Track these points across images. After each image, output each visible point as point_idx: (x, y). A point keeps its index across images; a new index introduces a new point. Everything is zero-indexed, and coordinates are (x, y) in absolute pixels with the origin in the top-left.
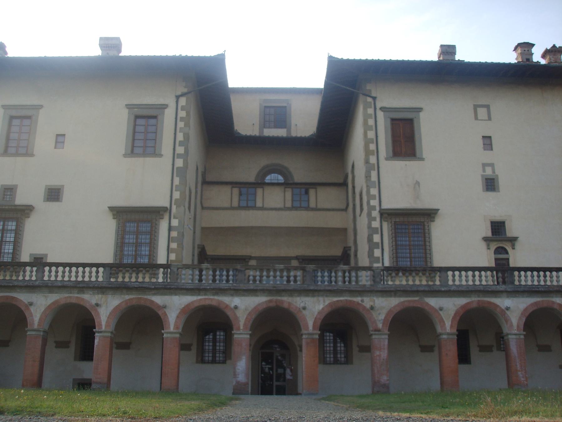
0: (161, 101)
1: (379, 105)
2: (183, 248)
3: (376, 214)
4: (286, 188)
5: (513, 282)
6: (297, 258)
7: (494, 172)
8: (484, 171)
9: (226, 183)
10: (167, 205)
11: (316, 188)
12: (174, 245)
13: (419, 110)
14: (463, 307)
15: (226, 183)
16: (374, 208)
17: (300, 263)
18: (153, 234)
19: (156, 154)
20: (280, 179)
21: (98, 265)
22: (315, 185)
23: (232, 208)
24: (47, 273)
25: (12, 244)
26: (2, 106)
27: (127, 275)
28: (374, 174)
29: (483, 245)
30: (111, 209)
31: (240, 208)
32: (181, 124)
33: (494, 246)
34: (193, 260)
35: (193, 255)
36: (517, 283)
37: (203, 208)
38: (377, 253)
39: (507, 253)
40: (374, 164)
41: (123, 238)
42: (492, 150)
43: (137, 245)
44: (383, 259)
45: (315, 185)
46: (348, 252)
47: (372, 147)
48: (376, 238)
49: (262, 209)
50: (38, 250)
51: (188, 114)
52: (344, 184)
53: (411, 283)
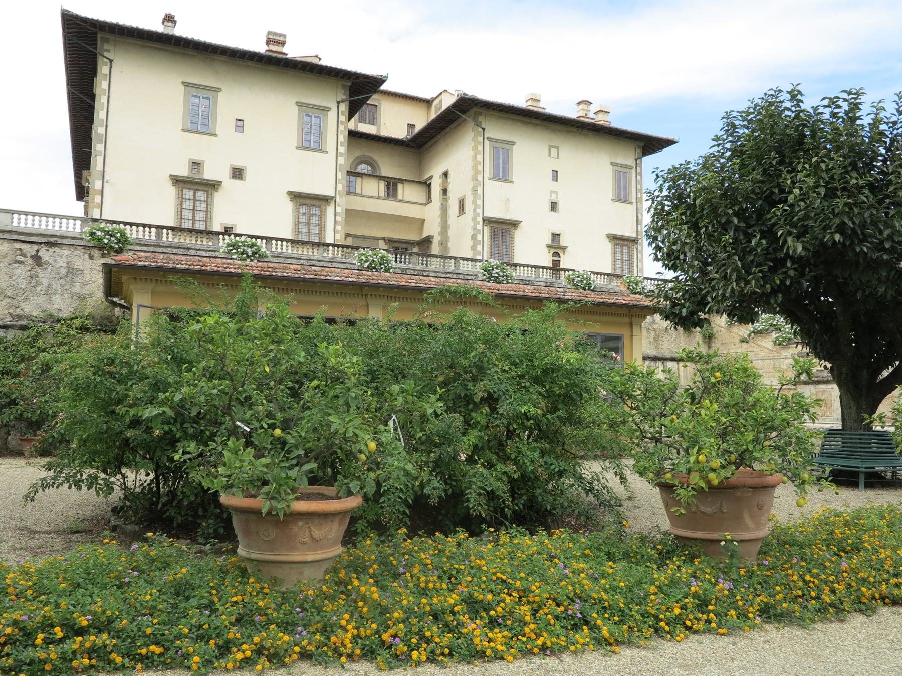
0: (324, 103)
3: (480, 219)
6: (384, 239)
8: (551, 197)
10: (333, 195)
13: (513, 143)
17: (386, 244)
18: (322, 217)
19: (320, 149)
22: (402, 181)
24: (274, 246)
26: (183, 82)
28: (480, 189)
29: (546, 250)
33: (552, 251)
38: (479, 248)
45: (402, 181)
47: (480, 168)
48: (479, 237)
49: (361, 195)
50: (229, 222)
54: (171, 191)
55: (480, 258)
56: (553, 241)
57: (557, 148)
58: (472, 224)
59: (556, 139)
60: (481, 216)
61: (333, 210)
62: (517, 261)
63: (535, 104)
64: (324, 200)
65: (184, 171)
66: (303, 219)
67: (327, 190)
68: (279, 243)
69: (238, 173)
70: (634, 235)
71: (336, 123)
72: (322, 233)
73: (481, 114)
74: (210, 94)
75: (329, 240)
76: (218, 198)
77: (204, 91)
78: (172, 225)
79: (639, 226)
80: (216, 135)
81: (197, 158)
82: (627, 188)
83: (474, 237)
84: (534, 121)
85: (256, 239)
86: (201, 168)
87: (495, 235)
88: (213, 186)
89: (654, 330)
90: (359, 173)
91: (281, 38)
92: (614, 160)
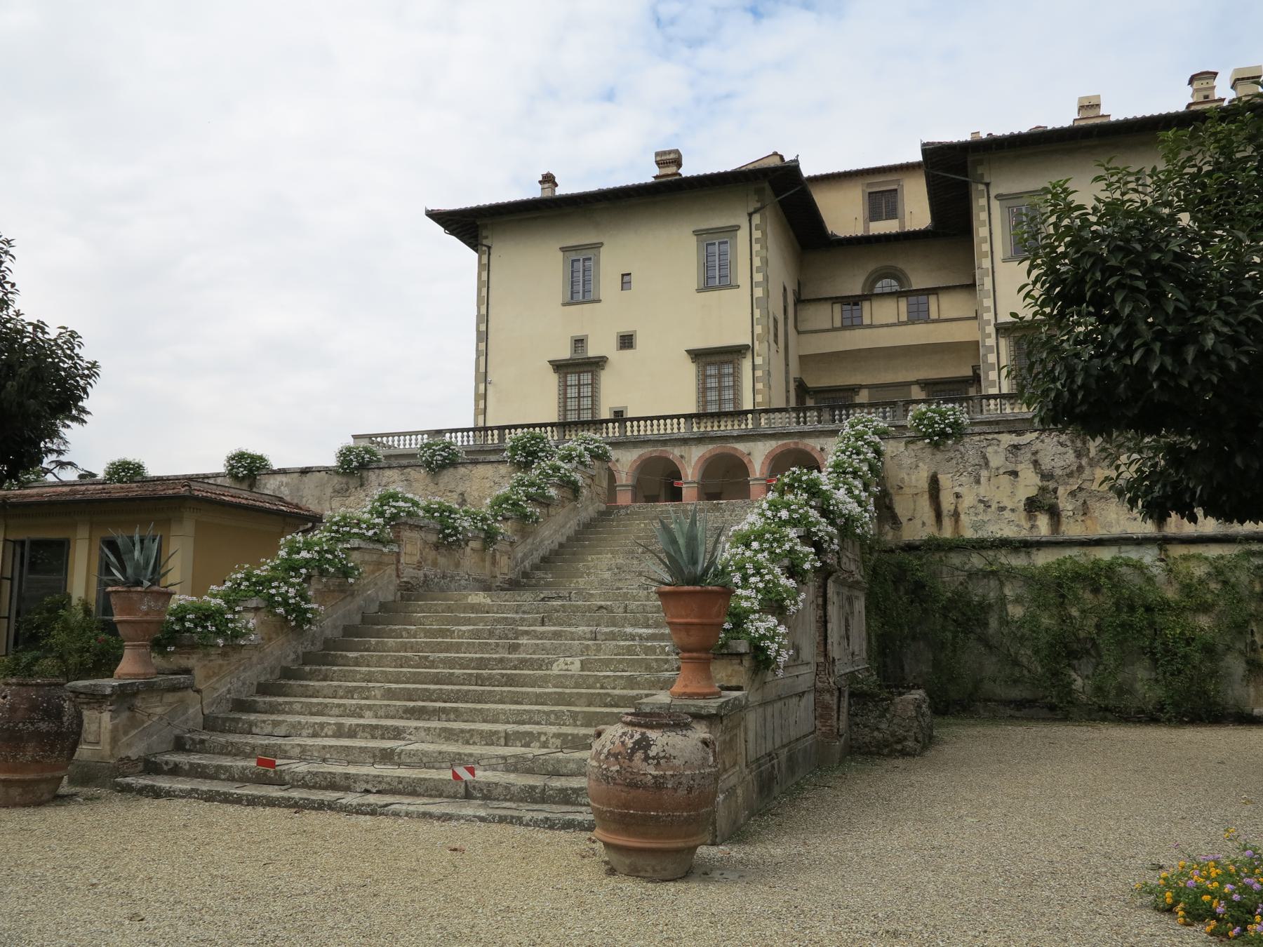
0: (732, 222)
1: (992, 194)
2: (770, 388)
3: (991, 329)
4: (898, 297)
6: (917, 382)
9: (826, 299)
11: (937, 294)
12: (759, 386)
15: (826, 299)
16: (988, 322)
17: (923, 389)
18: (736, 376)
20: (893, 285)
21: (678, 417)
23: (834, 329)
24: (629, 429)
25: (590, 399)
27: (709, 424)
30: (689, 352)
31: (844, 328)
32: (756, 247)
34: (788, 401)
35: (788, 391)
37: (799, 333)
40: (988, 269)
41: (704, 383)
43: (720, 389)
44: (1000, 383)
46: (977, 371)
49: (871, 326)
50: (618, 404)
51: (764, 233)
52: (971, 287)
54: (553, 379)
60: (993, 322)
61: (751, 363)
63: (1091, 113)
64: (733, 354)
65: (565, 353)
66: (712, 383)
67: (741, 337)
68: (662, 422)
69: (626, 341)
71: (749, 243)
72: (737, 399)
73: (981, 163)
74: (589, 254)
75: (747, 405)
76: (607, 379)
77: (584, 252)
78: (694, 411)
80: (599, 301)
81: (579, 333)
85: (382, 437)
86: (584, 345)
88: (598, 363)
90: (878, 295)
91: (672, 156)
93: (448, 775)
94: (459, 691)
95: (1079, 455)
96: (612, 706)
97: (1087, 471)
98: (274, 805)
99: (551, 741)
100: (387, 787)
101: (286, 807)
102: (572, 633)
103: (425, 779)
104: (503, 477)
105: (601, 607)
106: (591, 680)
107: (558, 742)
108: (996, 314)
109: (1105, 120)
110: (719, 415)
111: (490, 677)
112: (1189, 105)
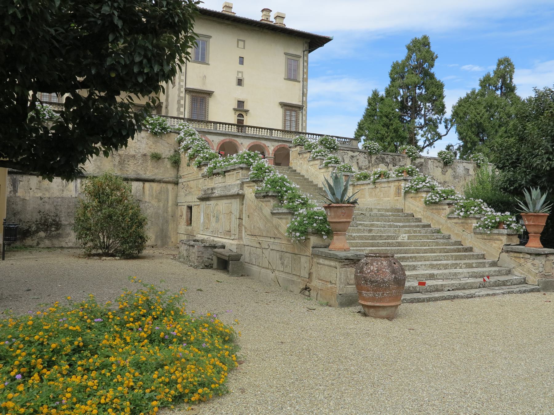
3: (183, 90)
5: (245, 132)
7: (242, 76)
8: (238, 75)
13: (210, 37)
14: (222, 141)
29: (233, 112)
33: (238, 113)
36: (247, 132)
38: (182, 110)
39: (243, 117)
42: (243, 64)
48: (182, 102)
53: (200, 127)
55: (182, 116)
56: (238, 106)
57: (244, 41)
58: (177, 92)
59: (243, 35)
62: (211, 119)
63: (228, 10)
70: (300, 104)
79: (304, 98)
82: (296, 70)
83: (179, 102)
84: (226, 22)
87: (194, 101)
89: (120, 155)
92: (287, 51)
93: (482, 280)
94: (398, 249)
95: (369, 163)
96: (447, 252)
97: (371, 168)
98: (437, 300)
99: (463, 266)
100: (455, 288)
101: (442, 300)
102: (377, 224)
103: (468, 283)
104: (143, 138)
105: (362, 214)
106: (425, 243)
107: (465, 266)
108: (186, 84)
109: (233, 14)
110: (290, 132)
111: (392, 243)
112: (262, 20)
